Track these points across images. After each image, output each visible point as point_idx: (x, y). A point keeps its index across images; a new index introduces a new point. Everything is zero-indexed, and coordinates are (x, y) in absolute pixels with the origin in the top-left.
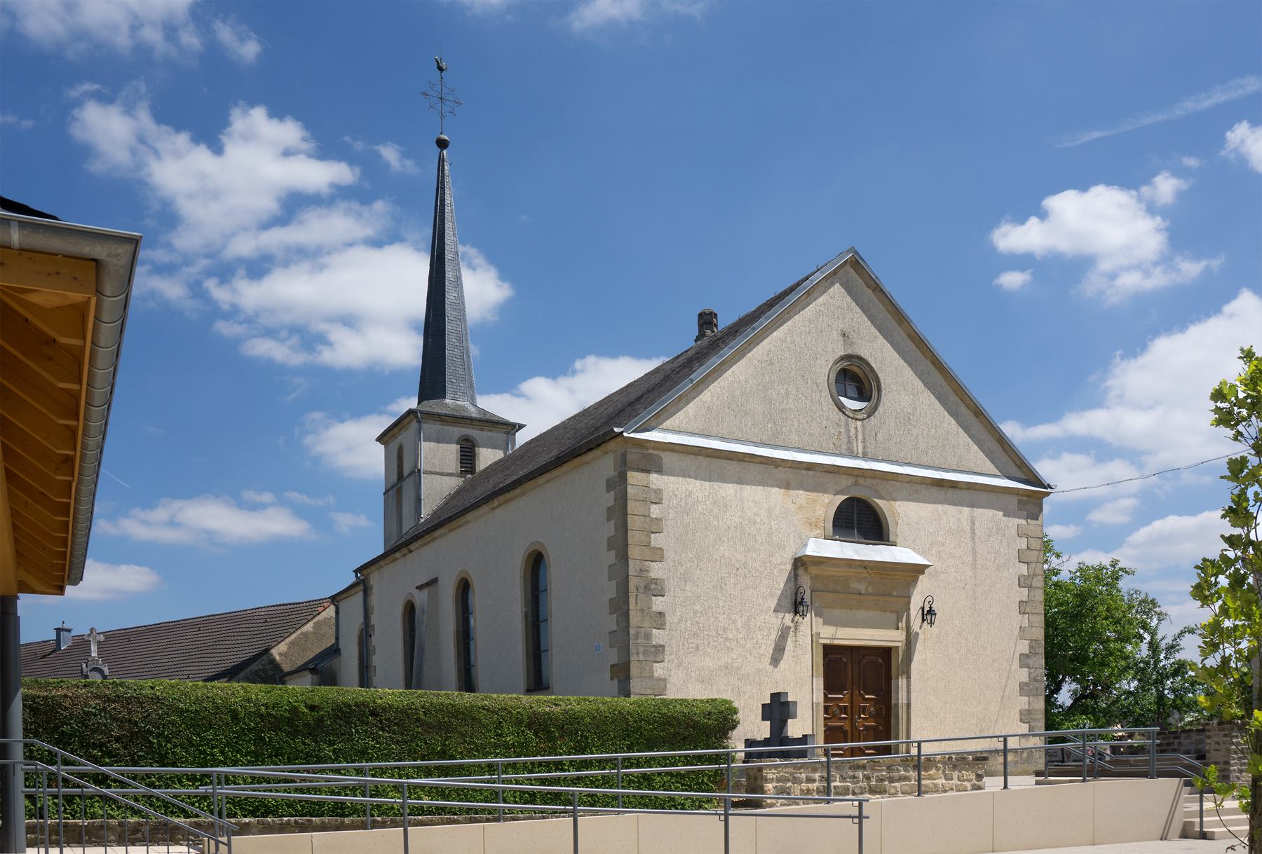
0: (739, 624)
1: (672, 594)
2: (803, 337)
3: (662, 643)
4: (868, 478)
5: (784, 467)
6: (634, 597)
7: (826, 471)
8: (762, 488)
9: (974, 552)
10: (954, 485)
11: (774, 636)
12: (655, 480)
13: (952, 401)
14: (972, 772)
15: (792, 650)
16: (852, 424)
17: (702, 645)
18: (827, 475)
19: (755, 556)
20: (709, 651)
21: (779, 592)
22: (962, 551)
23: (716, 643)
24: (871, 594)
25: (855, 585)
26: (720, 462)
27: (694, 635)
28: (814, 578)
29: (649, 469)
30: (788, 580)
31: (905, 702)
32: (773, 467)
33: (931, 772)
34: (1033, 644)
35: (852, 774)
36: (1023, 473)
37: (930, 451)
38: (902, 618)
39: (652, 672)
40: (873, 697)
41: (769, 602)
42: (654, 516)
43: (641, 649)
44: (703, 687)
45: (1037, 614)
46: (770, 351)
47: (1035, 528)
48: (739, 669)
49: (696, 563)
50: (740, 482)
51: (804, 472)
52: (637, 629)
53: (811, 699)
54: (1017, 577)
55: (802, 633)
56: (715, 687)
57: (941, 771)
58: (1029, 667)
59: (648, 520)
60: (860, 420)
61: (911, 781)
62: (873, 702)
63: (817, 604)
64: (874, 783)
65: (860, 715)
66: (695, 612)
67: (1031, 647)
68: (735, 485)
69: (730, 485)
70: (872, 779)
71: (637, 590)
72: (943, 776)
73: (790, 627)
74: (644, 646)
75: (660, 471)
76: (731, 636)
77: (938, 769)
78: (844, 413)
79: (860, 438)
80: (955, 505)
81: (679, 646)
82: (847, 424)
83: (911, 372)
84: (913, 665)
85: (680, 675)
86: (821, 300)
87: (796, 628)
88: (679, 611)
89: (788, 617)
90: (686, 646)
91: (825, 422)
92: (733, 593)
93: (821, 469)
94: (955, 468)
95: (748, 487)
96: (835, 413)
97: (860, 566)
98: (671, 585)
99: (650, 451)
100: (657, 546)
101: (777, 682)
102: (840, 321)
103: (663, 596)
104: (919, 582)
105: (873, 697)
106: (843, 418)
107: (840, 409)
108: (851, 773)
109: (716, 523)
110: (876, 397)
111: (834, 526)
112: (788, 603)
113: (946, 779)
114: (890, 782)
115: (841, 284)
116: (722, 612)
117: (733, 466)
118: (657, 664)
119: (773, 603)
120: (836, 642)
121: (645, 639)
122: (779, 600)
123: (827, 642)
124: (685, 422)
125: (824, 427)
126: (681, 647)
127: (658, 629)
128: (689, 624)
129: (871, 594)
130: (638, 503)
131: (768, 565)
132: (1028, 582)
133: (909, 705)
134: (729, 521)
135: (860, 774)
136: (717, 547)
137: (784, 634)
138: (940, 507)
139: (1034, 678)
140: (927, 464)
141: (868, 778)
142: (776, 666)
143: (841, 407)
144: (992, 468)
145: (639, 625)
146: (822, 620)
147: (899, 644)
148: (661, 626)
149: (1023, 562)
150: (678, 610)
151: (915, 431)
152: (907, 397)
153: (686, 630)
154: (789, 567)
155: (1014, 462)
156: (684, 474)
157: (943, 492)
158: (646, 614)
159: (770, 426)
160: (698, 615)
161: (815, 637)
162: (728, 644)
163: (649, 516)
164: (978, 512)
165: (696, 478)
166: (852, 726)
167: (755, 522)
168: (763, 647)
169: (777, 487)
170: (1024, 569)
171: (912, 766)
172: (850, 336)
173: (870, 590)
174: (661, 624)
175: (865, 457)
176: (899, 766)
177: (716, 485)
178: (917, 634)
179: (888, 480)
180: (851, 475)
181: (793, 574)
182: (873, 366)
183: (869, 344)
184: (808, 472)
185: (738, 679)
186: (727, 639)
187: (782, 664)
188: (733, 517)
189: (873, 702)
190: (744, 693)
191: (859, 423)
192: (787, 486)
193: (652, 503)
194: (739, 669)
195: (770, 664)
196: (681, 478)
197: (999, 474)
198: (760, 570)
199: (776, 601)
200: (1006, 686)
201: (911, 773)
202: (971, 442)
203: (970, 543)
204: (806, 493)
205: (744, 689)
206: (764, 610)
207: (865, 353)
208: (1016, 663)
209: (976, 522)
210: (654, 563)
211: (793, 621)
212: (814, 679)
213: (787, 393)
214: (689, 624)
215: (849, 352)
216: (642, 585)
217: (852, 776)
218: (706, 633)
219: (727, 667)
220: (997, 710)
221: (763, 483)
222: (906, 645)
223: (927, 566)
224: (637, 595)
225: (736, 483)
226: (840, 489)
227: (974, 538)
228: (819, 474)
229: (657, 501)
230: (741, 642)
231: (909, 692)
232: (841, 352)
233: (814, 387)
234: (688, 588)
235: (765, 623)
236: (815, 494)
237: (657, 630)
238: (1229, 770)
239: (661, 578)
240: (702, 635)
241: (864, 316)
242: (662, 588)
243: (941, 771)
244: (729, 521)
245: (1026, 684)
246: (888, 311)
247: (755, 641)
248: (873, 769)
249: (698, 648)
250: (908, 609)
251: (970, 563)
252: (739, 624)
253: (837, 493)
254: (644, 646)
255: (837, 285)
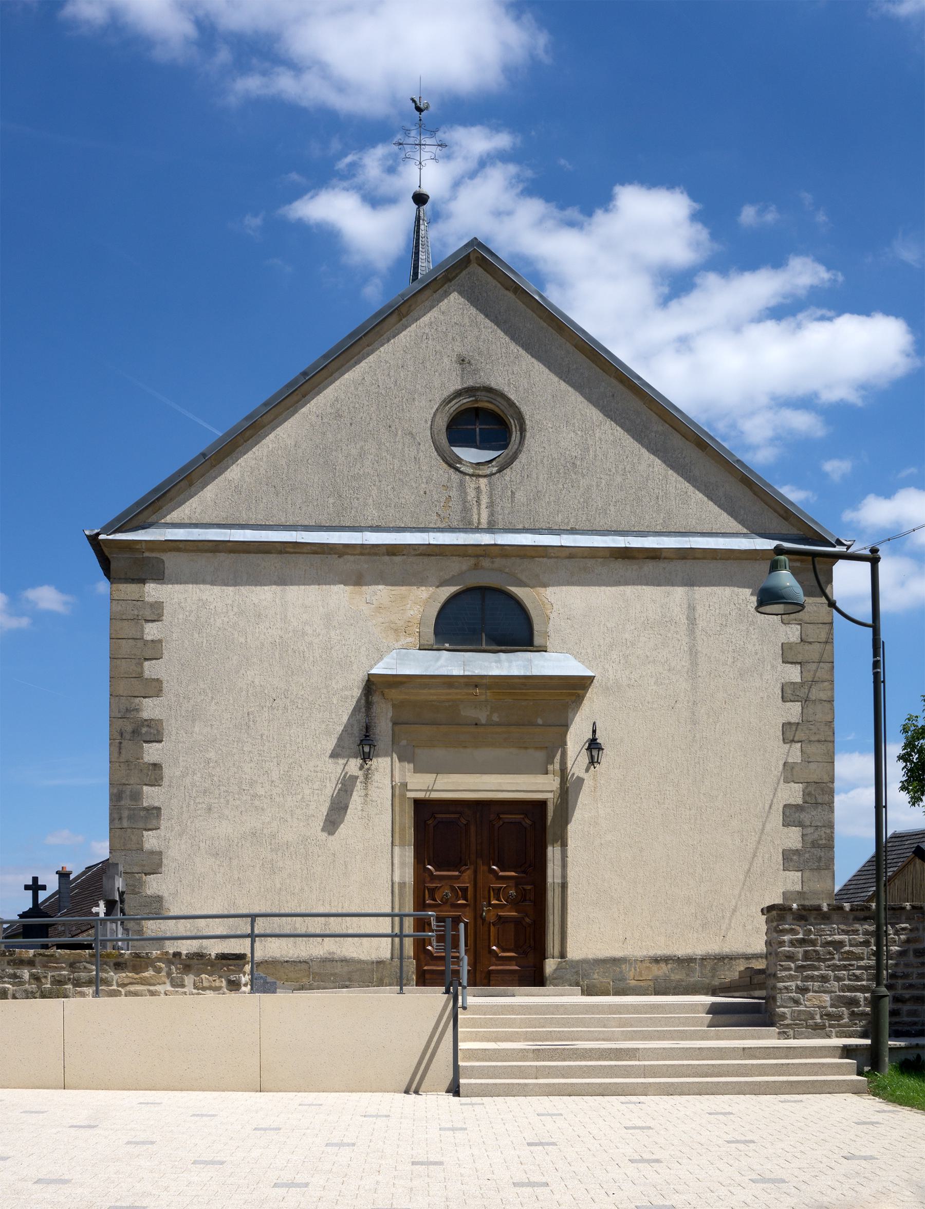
0: (275, 775)
1: (173, 738)
2: (392, 373)
3: (156, 805)
4: (496, 557)
5: (354, 555)
6: (117, 745)
7: (420, 555)
8: (317, 587)
9: (693, 652)
10: (654, 555)
11: (330, 789)
12: (153, 591)
13: (656, 432)
14: (220, 977)
15: (359, 808)
16: (471, 484)
17: (216, 805)
18: (426, 560)
19: (303, 680)
20: (226, 812)
21: (340, 729)
22: (670, 652)
23: (238, 802)
24: (498, 724)
25: (468, 713)
26: (252, 557)
27: (205, 791)
28: (397, 706)
29: (144, 577)
30: (356, 710)
31: (558, 880)
32: (337, 556)
33: (146, 974)
34: (809, 789)
35: (11, 971)
36: (793, 525)
37: (612, 508)
38: (554, 756)
39: (140, 843)
40: (513, 874)
41: (323, 742)
42: (149, 638)
43: (125, 813)
44: (218, 862)
45: (819, 741)
46: (337, 400)
47: (815, 608)
48: (274, 836)
49: (210, 695)
50: (282, 581)
51: (386, 558)
52: (120, 787)
53: (389, 877)
54: (779, 686)
55: (375, 784)
56: (235, 862)
57: (163, 973)
58: (800, 824)
59: (140, 644)
60: (485, 476)
61: (112, 985)
62: (512, 883)
63: (404, 742)
64: (49, 986)
65: (489, 901)
66: (208, 761)
67: (806, 794)
68: (274, 587)
69: (266, 588)
70: (43, 980)
71: (122, 736)
72: (168, 981)
73: (357, 777)
74: (129, 809)
75: (159, 577)
76: (261, 792)
77: (158, 971)
78: (457, 469)
79: (485, 500)
80: (659, 585)
81: (182, 807)
82: (462, 485)
83: (580, 399)
84: (571, 828)
85: (183, 846)
86: (426, 319)
87: (367, 777)
88: (183, 761)
89: (354, 766)
90: (192, 807)
91: (423, 486)
92: (266, 733)
93: (413, 552)
94: (658, 528)
95: (294, 588)
96: (441, 472)
97: (467, 685)
98: (171, 729)
99: (147, 554)
100: (153, 677)
101: (334, 855)
102: (457, 343)
103: (160, 741)
104: (586, 702)
105: (513, 874)
106: (455, 476)
107: (451, 466)
108: (10, 971)
109: (242, 640)
110: (517, 442)
111: (436, 633)
112: (352, 743)
113: (173, 986)
114: (75, 985)
115: (460, 293)
116: (248, 759)
117: (271, 562)
118: (150, 832)
119: (330, 744)
120: (435, 795)
121: (131, 800)
122: (340, 739)
123: (420, 795)
124: (198, 511)
125: (422, 493)
126: (185, 808)
127: (151, 785)
128: (197, 778)
129: (498, 724)
130: (125, 623)
131: (324, 691)
132: (802, 693)
133: (564, 886)
134: (262, 636)
135: (26, 974)
136: (243, 671)
137: (346, 787)
138: (629, 590)
139: (813, 842)
140: (606, 527)
141: (36, 978)
142: (331, 833)
143: (453, 463)
144: (733, 525)
145: (124, 781)
146: (412, 765)
147: (549, 796)
148: (156, 781)
149: (792, 663)
150: (181, 758)
151: (583, 482)
152: (572, 435)
153: (193, 785)
154: (357, 692)
155: (776, 511)
156: (196, 579)
157: (635, 567)
158: (133, 767)
159: (331, 500)
160: (211, 765)
161: (399, 790)
162: (257, 803)
163: (142, 638)
164: (701, 592)
165: (213, 583)
166: (475, 918)
167: (304, 634)
168: (313, 806)
169: (341, 583)
170: (794, 674)
171: (112, 964)
172: (472, 361)
173: (495, 718)
174: (156, 779)
175: (491, 529)
176: (87, 962)
177: (244, 590)
178: (580, 781)
179: (533, 557)
180: (465, 555)
181: (363, 701)
182: (512, 397)
183: (507, 368)
184: (394, 558)
185: (272, 850)
186: (255, 796)
187: (343, 830)
188: (269, 630)
189: (512, 883)
190: (281, 869)
191: (483, 482)
192: (358, 580)
193: (147, 621)
194: (274, 836)
195: (323, 830)
196: (191, 586)
197: (745, 531)
198: (310, 699)
199: (335, 741)
200: (754, 856)
201: (112, 974)
202: (691, 488)
203: (686, 639)
204: (390, 588)
205: (280, 864)
206: (314, 754)
207: (497, 381)
208: (777, 818)
209: (698, 607)
210: (147, 699)
211: (361, 768)
212: (397, 849)
213: (362, 454)
214: (197, 778)
215: (470, 383)
216: (129, 728)
217: (12, 974)
218: (223, 789)
219: (254, 834)
220: (737, 892)
221: (320, 580)
222: (561, 795)
223: (591, 679)
224: (120, 743)
225: (276, 583)
226: (447, 577)
227: (694, 633)
228: (411, 559)
229: (156, 618)
230: (277, 799)
231: (564, 866)
232: (456, 385)
233: (408, 439)
234: (197, 729)
235: (315, 771)
236: (404, 588)
237: (150, 788)
238: (774, 988)
239: (157, 718)
240: (217, 792)
241: (499, 331)
242: (158, 731)
243: (163, 973)
244: (262, 636)
245: (796, 852)
246: (541, 318)
247: (300, 797)
248: (44, 966)
249: (210, 809)
250: (564, 743)
251: (686, 669)
252: (275, 775)
253: (443, 583)
254: (129, 809)
255: (454, 296)
